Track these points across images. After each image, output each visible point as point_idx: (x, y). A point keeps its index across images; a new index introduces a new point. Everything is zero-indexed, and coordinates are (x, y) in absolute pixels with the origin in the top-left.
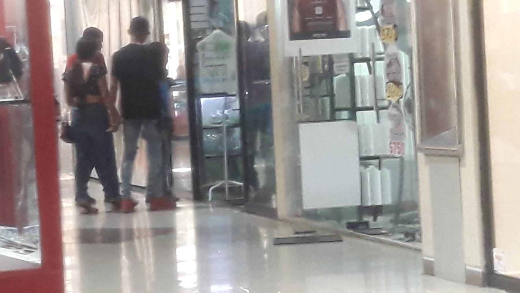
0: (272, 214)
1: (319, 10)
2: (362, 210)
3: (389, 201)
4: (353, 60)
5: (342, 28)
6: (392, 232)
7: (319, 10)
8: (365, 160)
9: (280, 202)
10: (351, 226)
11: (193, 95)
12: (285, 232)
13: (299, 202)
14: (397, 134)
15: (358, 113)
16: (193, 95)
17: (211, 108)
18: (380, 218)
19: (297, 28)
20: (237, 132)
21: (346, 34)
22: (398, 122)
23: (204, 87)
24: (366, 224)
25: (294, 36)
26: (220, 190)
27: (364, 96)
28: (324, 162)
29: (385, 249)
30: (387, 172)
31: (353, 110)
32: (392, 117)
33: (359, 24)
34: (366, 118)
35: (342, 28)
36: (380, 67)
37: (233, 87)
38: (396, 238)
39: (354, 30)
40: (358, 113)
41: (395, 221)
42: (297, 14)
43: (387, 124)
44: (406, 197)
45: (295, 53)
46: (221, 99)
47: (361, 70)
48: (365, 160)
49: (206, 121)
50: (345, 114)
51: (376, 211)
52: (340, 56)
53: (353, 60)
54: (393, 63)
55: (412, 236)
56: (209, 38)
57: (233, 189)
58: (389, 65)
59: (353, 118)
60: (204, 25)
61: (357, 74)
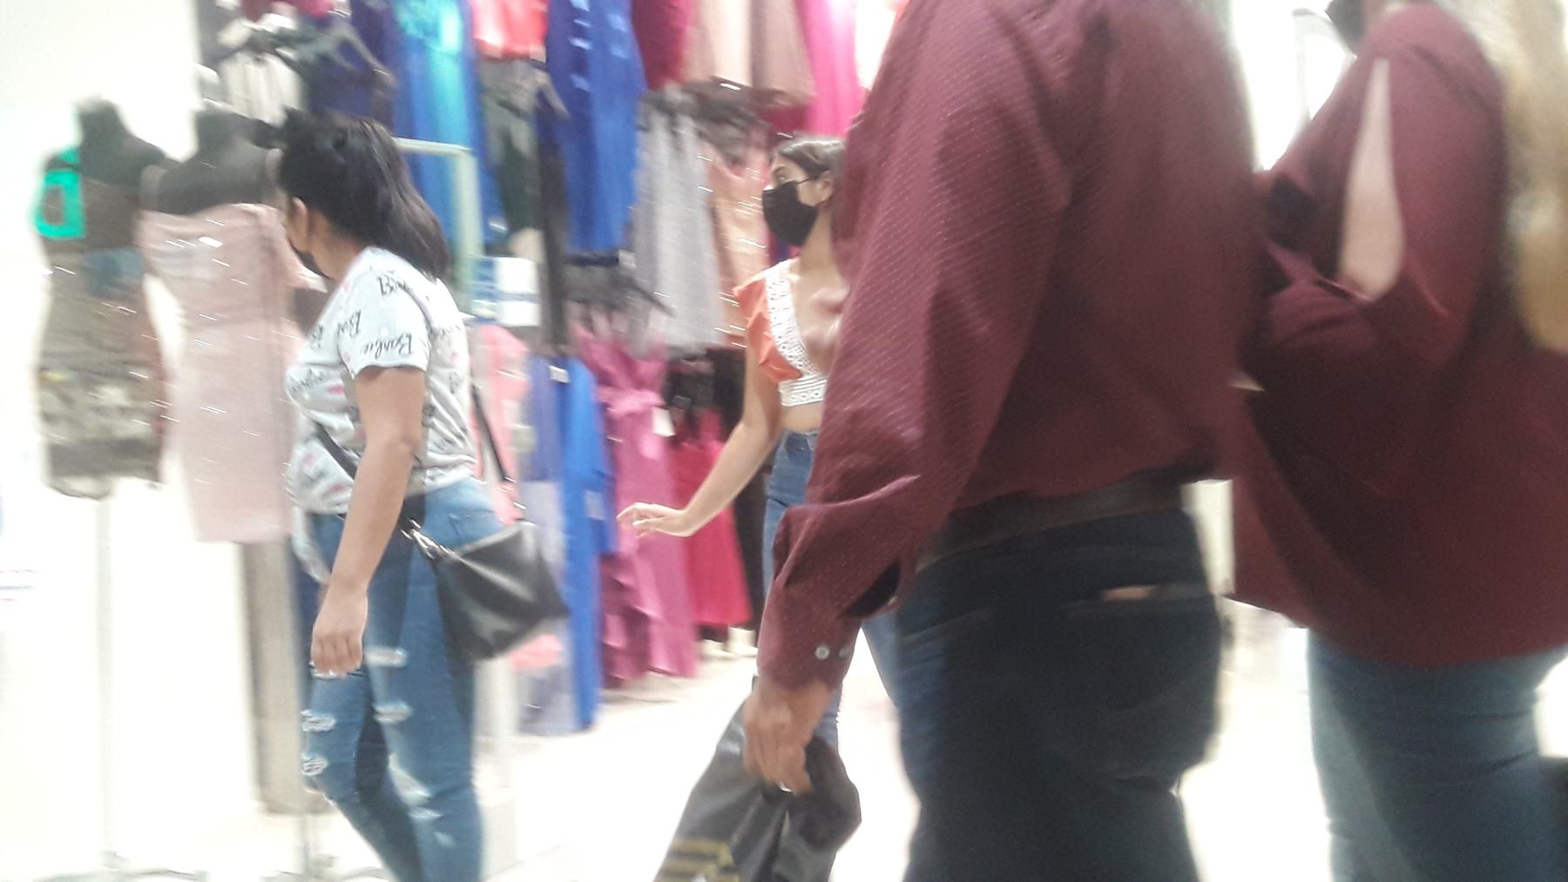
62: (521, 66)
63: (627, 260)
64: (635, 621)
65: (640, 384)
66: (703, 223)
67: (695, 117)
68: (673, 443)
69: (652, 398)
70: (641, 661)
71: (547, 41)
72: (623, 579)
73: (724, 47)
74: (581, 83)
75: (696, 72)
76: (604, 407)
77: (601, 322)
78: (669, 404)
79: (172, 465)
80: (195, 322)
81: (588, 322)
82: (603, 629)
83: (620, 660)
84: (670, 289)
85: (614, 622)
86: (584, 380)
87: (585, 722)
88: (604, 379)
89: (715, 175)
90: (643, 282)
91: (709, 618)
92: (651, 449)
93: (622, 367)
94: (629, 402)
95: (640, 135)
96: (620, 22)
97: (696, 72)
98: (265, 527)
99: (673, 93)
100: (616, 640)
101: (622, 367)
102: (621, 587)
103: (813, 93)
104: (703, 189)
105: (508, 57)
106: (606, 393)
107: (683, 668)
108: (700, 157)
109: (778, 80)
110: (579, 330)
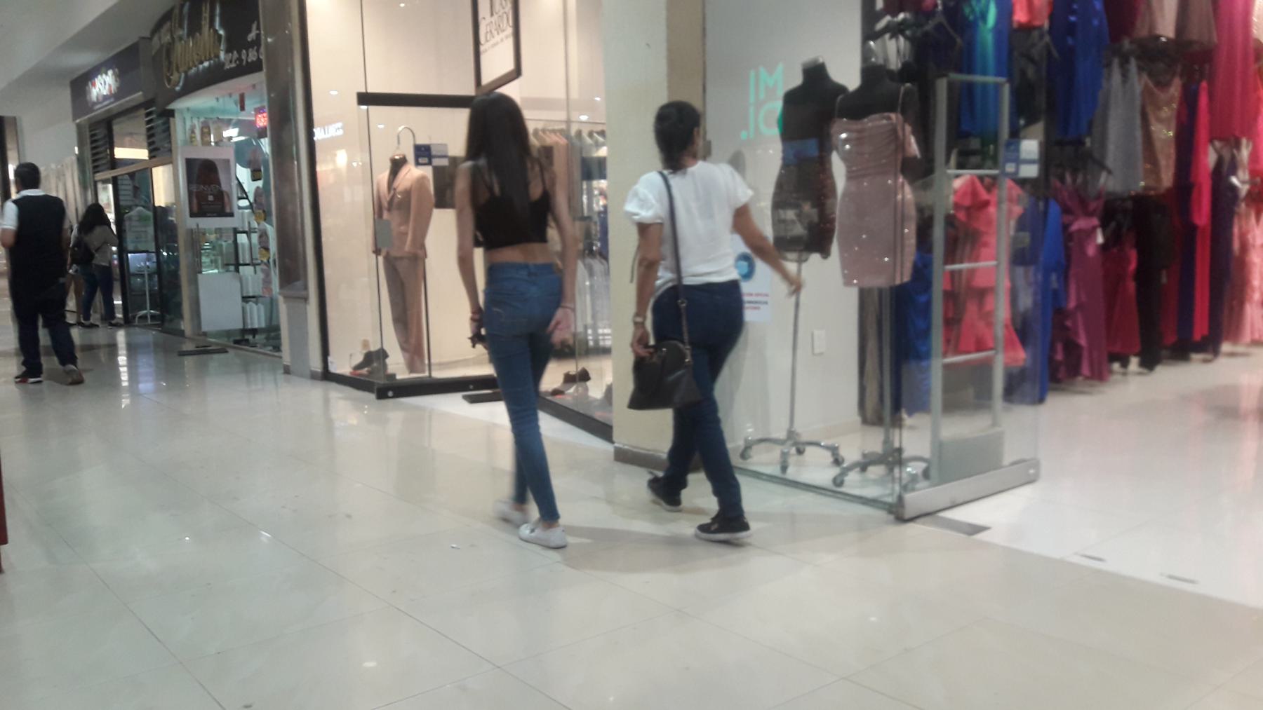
0: (181, 333)
1: (211, 198)
2: (244, 331)
3: (263, 325)
4: (236, 232)
5: (228, 210)
6: (264, 346)
7: (211, 198)
8: (246, 299)
9: (186, 325)
10: (236, 342)
11: (122, 252)
12: (189, 346)
13: (199, 325)
14: (267, 282)
15: (241, 268)
16: (122, 252)
17: (136, 260)
18: (257, 337)
19: (195, 209)
20: (156, 278)
21: (231, 215)
22: (267, 274)
23: (130, 247)
24: (247, 340)
25: (192, 215)
26: (144, 317)
27: (244, 256)
28: (218, 298)
29: (260, 356)
30: (262, 307)
31: (237, 265)
32: (263, 270)
33: (240, 208)
34: (246, 271)
35: (228, 210)
36: (255, 237)
37: (152, 247)
38: (268, 350)
39: (236, 210)
40: (241, 268)
41: (267, 338)
42: (195, 201)
43: (261, 275)
44: (274, 323)
45: (194, 227)
46: (144, 255)
47: (242, 239)
48: (246, 299)
49: (132, 270)
50: (232, 268)
51: (254, 332)
52: (227, 229)
53: (236, 232)
54: (263, 236)
55: (277, 348)
56: (133, 213)
57: (153, 317)
58: (260, 237)
59: (237, 270)
60: (129, 203)
61: (239, 241)
62: (1036, 34)
63: (1088, 142)
64: (1072, 348)
65: (1089, 214)
66: (1138, 121)
67: (1138, 58)
68: (1104, 247)
69: (1095, 221)
70: (1074, 371)
71: (1052, 17)
72: (1069, 323)
73: (1165, 16)
74: (1070, 41)
75: (1142, 31)
76: (1065, 227)
77: (1069, 179)
78: (1104, 226)
79: (835, 248)
80: (851, 176)
81: (1062, 179)
82: (1052, 349)
83: (1062, 370)
84: (1112, 157)
85: (1059, 347)
86: (1055, 209)
87: (1041, 400)
88: (1066, 210)
89: (1147, 92)
90: (1096, 155)
91: (1117, 349)
92: (1091, 251)
93: (1080, 203)
94: (1080, 224)
95: (1105, 71)
96: (1099, 5)
97: (1142, 31)
98: (879, 281)
99: (1126, 44)
100: (1059, 356)
101: (1080, 203)
102: (1067, 329)
103: (1215, 39)
104: (1138, 103)
105: (1026, 29)
106: (1067, 219)
107: (1099, 375)
108: (1138, 82)
109: (1194, 33)
110: (1055, 182)
